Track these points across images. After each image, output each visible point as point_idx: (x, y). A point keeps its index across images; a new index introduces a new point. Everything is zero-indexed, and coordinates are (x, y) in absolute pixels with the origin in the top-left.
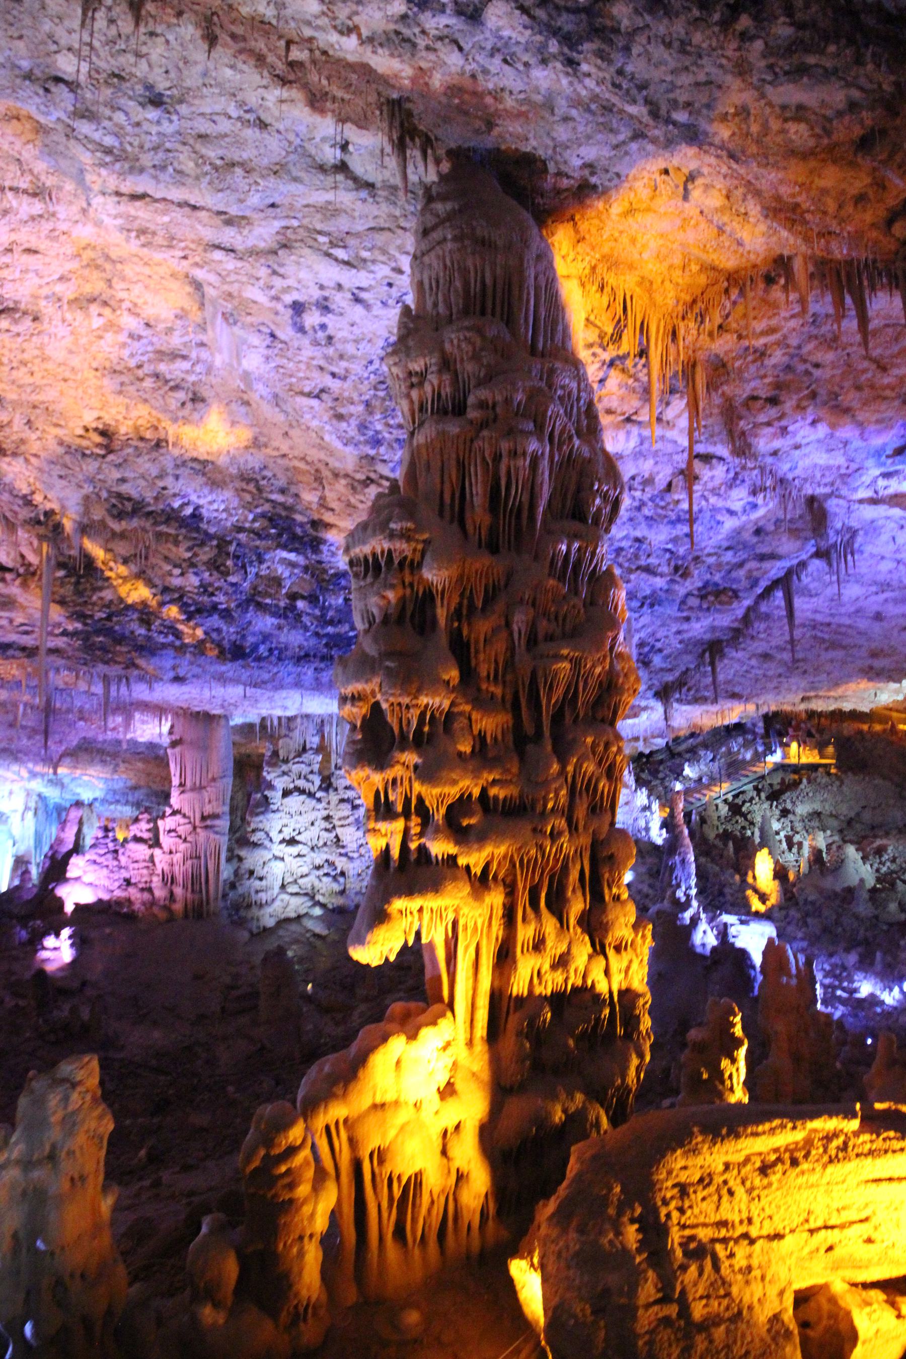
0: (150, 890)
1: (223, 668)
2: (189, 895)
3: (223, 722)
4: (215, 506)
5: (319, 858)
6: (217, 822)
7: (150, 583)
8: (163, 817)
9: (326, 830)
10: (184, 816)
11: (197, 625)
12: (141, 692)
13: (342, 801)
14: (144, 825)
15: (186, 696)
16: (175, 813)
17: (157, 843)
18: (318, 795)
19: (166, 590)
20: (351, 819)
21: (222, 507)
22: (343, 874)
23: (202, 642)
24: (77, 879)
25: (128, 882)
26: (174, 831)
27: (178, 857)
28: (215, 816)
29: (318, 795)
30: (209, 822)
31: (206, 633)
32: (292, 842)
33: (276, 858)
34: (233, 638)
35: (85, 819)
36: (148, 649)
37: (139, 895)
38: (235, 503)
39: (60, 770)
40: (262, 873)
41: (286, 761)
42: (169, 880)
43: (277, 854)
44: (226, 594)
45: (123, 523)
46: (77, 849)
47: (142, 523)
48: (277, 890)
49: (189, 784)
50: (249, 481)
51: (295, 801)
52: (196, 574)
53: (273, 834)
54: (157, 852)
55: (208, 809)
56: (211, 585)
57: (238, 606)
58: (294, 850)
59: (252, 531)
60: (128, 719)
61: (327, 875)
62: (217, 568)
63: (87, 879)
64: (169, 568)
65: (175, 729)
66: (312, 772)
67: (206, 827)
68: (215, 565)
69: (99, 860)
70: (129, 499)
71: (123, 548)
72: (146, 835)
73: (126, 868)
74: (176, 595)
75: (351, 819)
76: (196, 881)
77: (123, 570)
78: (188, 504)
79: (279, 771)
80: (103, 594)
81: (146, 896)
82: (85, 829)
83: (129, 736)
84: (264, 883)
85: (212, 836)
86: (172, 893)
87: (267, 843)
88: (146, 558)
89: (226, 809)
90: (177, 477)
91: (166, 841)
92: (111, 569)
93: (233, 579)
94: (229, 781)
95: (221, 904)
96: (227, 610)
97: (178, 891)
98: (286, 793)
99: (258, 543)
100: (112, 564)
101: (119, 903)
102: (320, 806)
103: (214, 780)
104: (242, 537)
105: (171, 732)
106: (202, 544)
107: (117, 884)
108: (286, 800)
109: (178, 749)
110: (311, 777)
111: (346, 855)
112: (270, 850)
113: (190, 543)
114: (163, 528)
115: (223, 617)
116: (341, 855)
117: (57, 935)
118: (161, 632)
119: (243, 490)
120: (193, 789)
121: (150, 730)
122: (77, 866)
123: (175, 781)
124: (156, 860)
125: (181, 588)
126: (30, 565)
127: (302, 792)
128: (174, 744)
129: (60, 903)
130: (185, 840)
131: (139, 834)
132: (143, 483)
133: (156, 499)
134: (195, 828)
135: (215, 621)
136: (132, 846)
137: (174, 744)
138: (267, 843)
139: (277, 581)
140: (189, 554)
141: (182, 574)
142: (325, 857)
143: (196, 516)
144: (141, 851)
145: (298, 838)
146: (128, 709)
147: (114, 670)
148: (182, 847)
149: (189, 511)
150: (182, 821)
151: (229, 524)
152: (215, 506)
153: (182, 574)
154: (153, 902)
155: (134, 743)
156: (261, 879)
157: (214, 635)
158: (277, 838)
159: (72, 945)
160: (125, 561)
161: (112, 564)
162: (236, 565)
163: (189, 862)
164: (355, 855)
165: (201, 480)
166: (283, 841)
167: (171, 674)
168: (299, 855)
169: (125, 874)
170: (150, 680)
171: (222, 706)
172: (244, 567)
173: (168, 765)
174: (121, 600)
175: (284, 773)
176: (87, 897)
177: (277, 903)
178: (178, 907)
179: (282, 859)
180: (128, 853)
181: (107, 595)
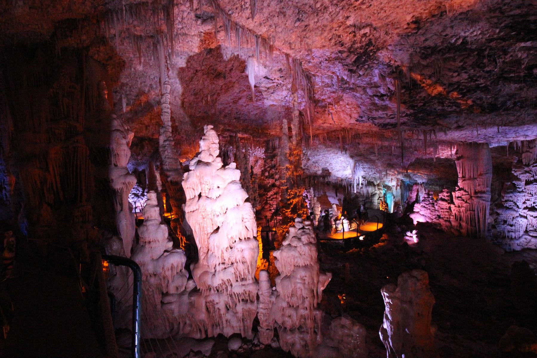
0: (450, 222)
1: (484, 118)
2: (469, 227)
3: (485, 147)
4: (475, 33)
6: (484, 195)
7: (442, 84)
8: (454, 191)
10: (465, 191)
11: (468, 99)
12: (441, 136)
14: (445, 194)
15: (464, 136)
16: (460, 189)
17: (452, 202)
19: (450, 85)
21: (479, 32)
23: (472, 106)
24: (418, 212)
25: (439, 217)
26: (460, 197)
27: (462, 209)
28: (483, 192)
30: (479, 195)
31: (473, 101)
33: (521, 216)
34: (490, 101)
35: (419, 190)
36: (444, 115)
37: (444, 223)
38: (487, 26)
39: (409, 171)
40: (512, 223)
41: (528, 166)
42: (458, 218)
43: (521, 214)
44: (484, 78)
45: (428, 60)
46: (417, 201)
47: (436, 57)
48: (522, 233)
49: (467, 176)
50: (494, 11)
52: (466, 73)
53: (520, 204)
54: (452, 206)
55: (478, 189)
56: (474, 76)
57: (491, 83)
59: (498, 38)
60: (436, 149)
62: (478, 66)
63: (421, 213)
64: (451, 74)
65: (459, 152)
67: (478, 197)
68: (478, 65)
69: (426, 206)
70: (429, 48)
71: (428, 72)
72: (446, 198)
73: (438, 211)
74: (456, 86)
76: (472, 221)
77: (429, 82)
78: (460, 38)
79: (523, 171)
80: (421, 95)
81: (447, 223)
82: (420, 194)
83: (436, 156)
84: (513, 228)
85: (481, 202)
86: (460, 225)
87: (515, 208)
88: (440, 73)
89: (489, 189)
90: (452, 27)
91: (456, 202)
92: (424, 83)
93: (487, 69)
94: (489, 177)
95: (486, 234)
96: (485, 87)
97: (464, 224)
98: (528, 183)
99: (503, 44)
100: (424, 80)
101: (435, 224)
103: (481, 175)
104: (491, 44)
105: (456, 153)
106: (469, 55)
107: (434, 217)
108: (527, 187)
109: (460, 161)
112: (517, 211)
113: (462, 58)
114: (448, 55)
115: (482, 91)
117: (411, 232)
118: (449, 106)
119: (492, 17)
120: (470, 179)
121: (446, 153)
122: (417, 207)
123: (460, 175)
124: (452, 209)
125: (458, 82)
126: (392, 91)
128: (458, 159)
129: (412, 220)
130: (466, 202)
131: (443, 198)
132: (435, 37)
133: (442, 42)
134: (471, 197)
135: (479, 94)
136: (440, 202)
137: (458, 159)
138: (515, 208)
139: (518, 62)
140: (462, 64)
141: (458, 75)
143: (465, 42)
144: (445, 205)
146: (436, 144)
147: (429, 127)
148: (465, 205)
149: (460, 41)
150: (464, 193)
151: (484, 40)
152: (475, 33)
153: (458, 75)
154: (452, 227)
155: (438, 158)
156: (511, 226)
157: (478, 102)
159: (417, 237)
160: (430, 77)
161: (424, 80)
162: (489, 61)
163: (469, 212)
165: (466, 22)
166: (526, 208)
167: (455, 125)
169: (437, 213)
170: (445, 129)
171: (485, 139)
172: (495, 61)
173: (456, 169)
174: (429, 95)
175: (526, 172)
176: (422, 220)
177: (522, 240)
178: (463, 231)
180: (438, 205)
181: (423, 94)
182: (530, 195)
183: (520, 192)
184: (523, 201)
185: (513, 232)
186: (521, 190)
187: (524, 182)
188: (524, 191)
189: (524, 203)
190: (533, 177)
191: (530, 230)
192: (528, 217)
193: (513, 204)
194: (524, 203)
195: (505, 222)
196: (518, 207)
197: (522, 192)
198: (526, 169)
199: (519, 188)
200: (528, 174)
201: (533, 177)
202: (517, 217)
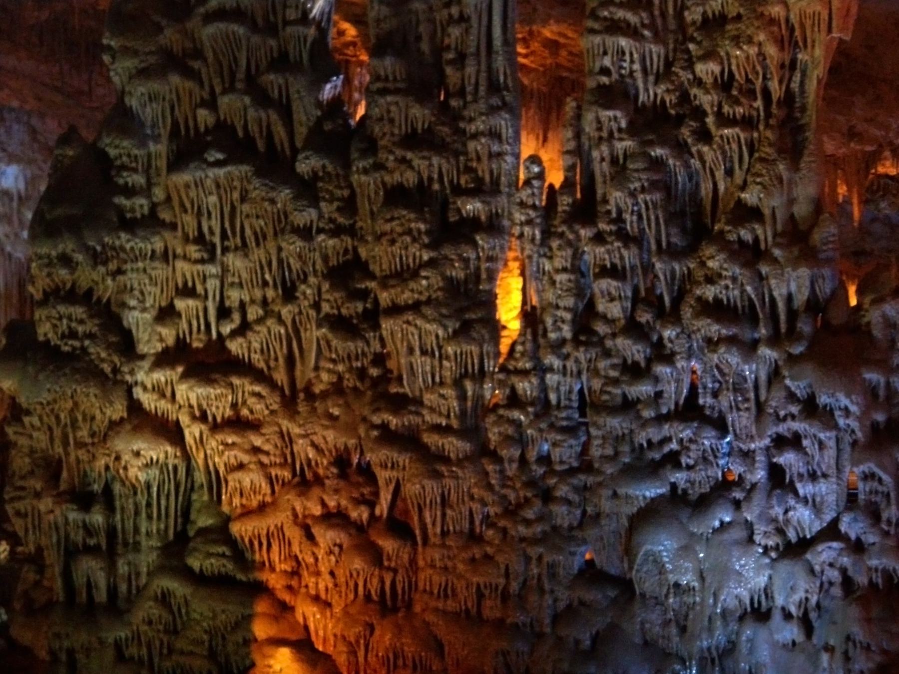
5: (316, 440)
9: (340, 324)
13: (396, 196)
18: (305, 165)
20: (428, 283)
22: (398, 526)
29: (305, 165)
32: (206, 362)
33: (141, 420)
43: (148, 400)
48: (147, 559)
51: (208, 184)
53: (138, 319)
58: (215, 397)
61: (334, 518)
66: (281, 62)
75: (428, 283)
84: (97, 518)
98: (187, 150)
102: (305, 216)
108: (183, 178)
110: (272, 80)
111: (407, 440)
112: (112, 382)
116: (388, 436)
127: (236, 145)
142: (331, 438)
145: (235, 347)
158: (152, 338)
164: (454, 446)
168: (238, 423)
175: (173, 62)
177: (147, 609)
179: (171, 432)
182: (193, 251)
183: (130, 225)
184: (155, 297)
185: (92, 551)
186: (140, 205)
187: (160, 149)
188: (165, 215)
189: (167, 314)
190: (211, 104)
191: (202, 532)
192: (184, 420)
193: (91, 326)
194: (167, 314)
195: (51, 469)
196: (127, 346)
197: (152, 222)
198: (170, 36)
199: (130, 192)
200: (175, 79)
201: (211, 104)
202: (114, 425)
